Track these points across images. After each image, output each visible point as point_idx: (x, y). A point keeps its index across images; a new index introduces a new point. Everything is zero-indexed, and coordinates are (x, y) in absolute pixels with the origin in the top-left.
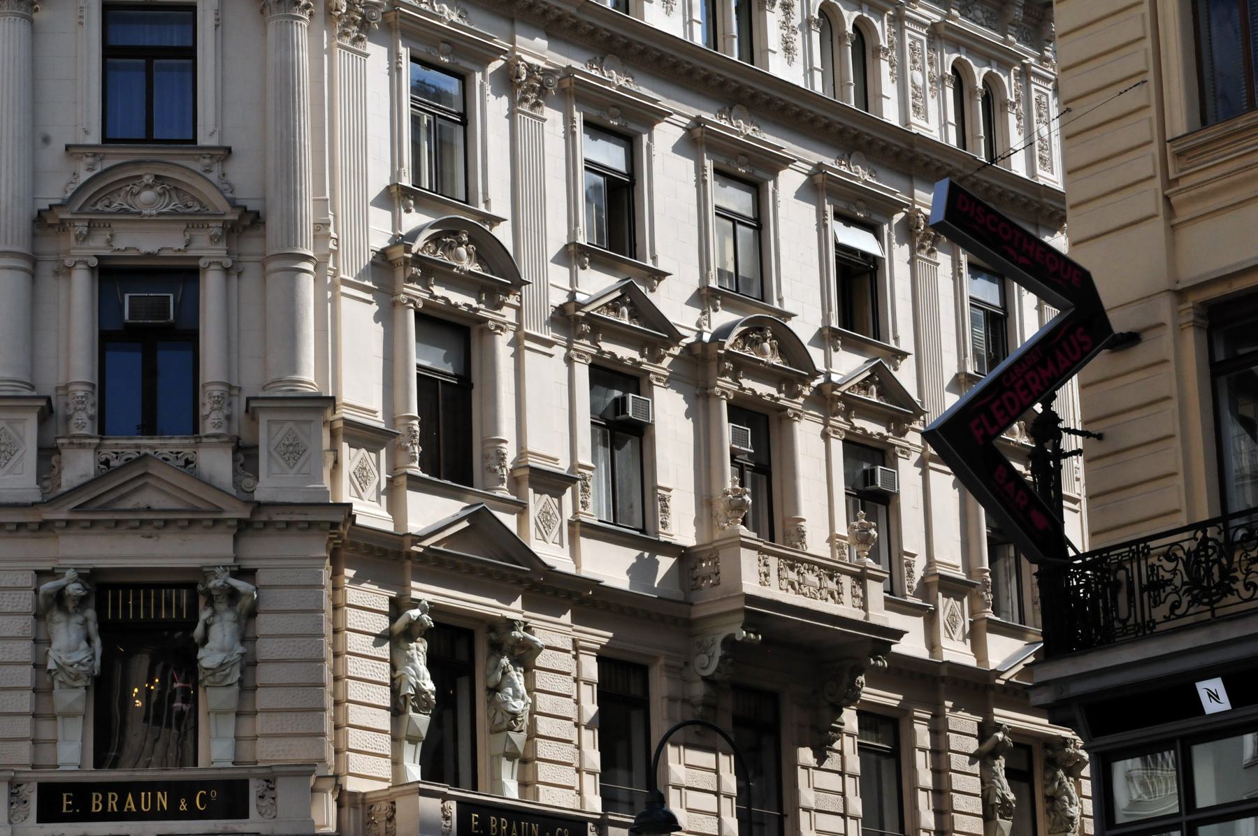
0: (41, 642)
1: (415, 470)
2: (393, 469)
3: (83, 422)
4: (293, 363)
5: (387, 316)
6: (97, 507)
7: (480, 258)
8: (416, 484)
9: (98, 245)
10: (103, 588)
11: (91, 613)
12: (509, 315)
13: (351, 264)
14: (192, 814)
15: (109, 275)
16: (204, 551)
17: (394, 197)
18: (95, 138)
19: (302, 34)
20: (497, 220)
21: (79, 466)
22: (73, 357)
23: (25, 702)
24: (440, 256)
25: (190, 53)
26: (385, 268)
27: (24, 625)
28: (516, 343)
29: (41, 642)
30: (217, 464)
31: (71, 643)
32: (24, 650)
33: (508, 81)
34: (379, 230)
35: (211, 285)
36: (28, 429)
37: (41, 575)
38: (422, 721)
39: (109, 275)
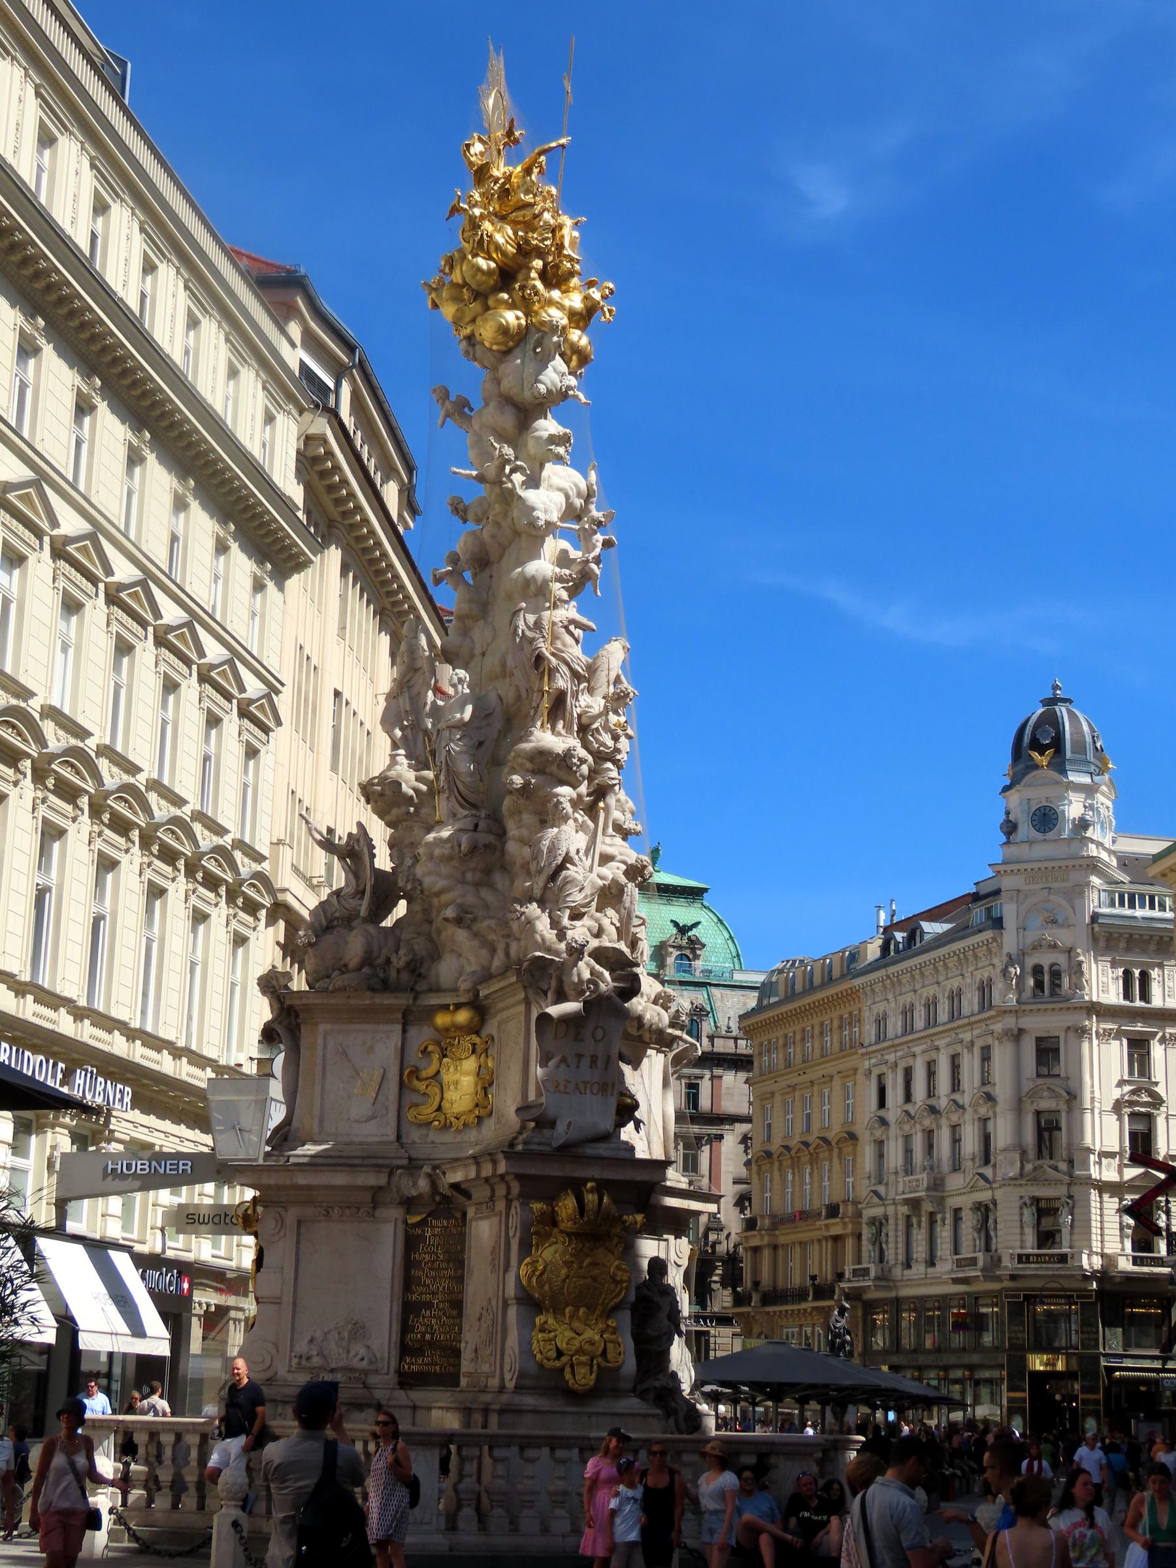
0: (1021, 1215)
1: (1126, 1162)
2: (1121, 1160)
3: (1032, 1154)
4: (1082, 1138)
5: (1120, 1119)
6: (1035, 1178)
7: (1150, 1096)
8: (1127, 1166)
9: (1035, 1107)
10: (1036, 1200)
11: (1034, 1208)
12: (1163, 1109)
13: (1108, 1106)
14: (1054, 1262)
15: (1038, 1113)
16: (1060, 1191)
17: (1121, 1083)
18: (1034, 1075)
19: (1085, 1045)
20: (1157, 1084)
21: (1029, 1167)
22: (1030, 1138)
23: (1018, 1231)
24: (1135, 1098)
25: (1057, 1050)
26: (1118, 1107)
27: (1017, 1211)
28: (1167, 1118)
29: (1021, 1215)
30: (1063, 1166)
31: (1029, 1215)
32: (1017, 1217)
33: (1163, 1040)
34: (1117, 1093)
35: (1064, 1115)
36: (1017, 1156)
37: (1021, 1197)
38: (1129, 1232)
39: (1038, 1113)
